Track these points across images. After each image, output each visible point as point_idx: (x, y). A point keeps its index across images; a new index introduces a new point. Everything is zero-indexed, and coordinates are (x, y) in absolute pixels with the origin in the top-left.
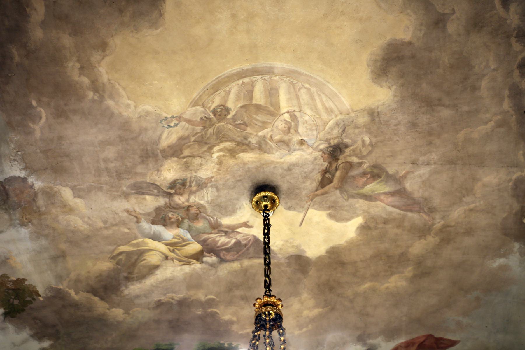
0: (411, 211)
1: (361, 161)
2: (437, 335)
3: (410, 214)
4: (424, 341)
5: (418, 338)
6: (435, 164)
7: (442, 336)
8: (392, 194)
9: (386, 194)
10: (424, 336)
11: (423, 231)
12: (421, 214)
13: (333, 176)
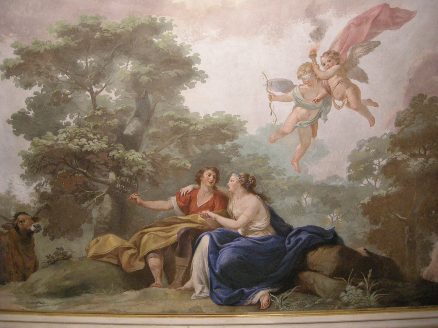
2: (392, 6)
5: (372, 10)
10: (379, 7)
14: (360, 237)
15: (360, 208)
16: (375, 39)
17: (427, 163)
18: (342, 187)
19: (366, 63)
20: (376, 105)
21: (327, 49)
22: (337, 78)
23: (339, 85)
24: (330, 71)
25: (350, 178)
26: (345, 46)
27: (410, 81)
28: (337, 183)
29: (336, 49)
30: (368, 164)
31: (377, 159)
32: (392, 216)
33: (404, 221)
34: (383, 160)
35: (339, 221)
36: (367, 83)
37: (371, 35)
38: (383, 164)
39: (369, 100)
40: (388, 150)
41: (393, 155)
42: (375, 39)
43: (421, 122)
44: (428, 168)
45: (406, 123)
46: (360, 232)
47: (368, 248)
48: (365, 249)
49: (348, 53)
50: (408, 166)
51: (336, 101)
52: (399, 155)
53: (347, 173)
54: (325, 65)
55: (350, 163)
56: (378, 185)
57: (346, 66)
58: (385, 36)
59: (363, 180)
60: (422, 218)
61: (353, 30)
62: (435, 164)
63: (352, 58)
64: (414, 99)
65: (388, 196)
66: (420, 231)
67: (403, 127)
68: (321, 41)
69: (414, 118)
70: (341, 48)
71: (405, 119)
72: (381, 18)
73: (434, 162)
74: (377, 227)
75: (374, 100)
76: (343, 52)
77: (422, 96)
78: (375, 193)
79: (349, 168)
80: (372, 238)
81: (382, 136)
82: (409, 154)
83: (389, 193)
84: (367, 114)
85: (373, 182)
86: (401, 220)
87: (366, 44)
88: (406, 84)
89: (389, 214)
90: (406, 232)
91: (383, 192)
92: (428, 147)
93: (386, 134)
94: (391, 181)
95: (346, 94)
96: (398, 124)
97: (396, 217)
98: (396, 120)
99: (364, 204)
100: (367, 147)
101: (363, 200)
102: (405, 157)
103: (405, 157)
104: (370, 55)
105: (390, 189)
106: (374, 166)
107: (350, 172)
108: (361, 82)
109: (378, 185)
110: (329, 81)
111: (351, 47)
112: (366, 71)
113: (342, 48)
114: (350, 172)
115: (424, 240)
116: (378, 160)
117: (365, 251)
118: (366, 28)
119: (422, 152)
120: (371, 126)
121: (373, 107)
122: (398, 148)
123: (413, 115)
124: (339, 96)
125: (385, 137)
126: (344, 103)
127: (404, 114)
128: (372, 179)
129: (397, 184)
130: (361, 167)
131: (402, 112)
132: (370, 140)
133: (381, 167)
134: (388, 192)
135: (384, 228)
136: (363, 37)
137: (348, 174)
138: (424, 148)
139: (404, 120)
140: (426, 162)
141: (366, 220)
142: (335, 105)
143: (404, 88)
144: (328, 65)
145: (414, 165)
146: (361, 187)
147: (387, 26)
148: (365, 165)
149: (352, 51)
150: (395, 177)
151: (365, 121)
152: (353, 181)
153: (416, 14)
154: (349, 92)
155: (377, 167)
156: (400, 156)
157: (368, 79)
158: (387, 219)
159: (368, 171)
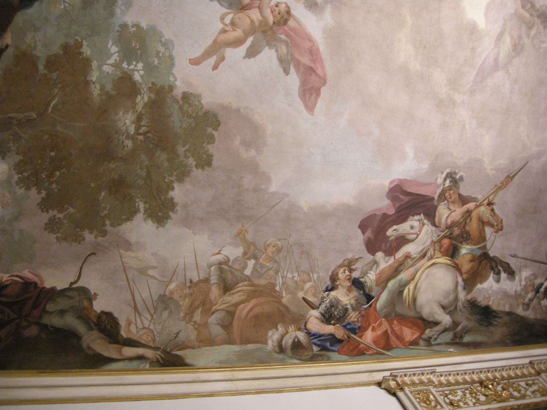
0: (477, 74)
1: (531, 37)
2: (323, 90)
3: (475, 72)
4: (317, 74)
5: (323, 68)
6: (510, 97)
7: (322, 95)
8: (496, 60)
9: (498, 54)
10: (325, 75)
11: (454, 83)
12: (471, 83)
13: (527, 11)
14: (29, 39)
15: (77, 40)
16: (292, 70)
17: (126, 138)
18: (112, 14)
19: (268, 57)
20: (215, 67)
21: (293, 12)
22: (258, 20)
23: (250, 22)
24: (268, 13)
25: (124, 26)
26: (292, 34)
27: (238, 110)
28: (120, 6)
29: (291, 23)
30: (139, 55)
31: (143, 67)
32: (56, 91)
33: (46, 110)
34: (141, 77)
35: (61, 5)
36: (244, 58)
37: (298, 65)
38: (135, 76)
39: (223, 59)
40: (153, 83)
41: (145, 89)
42: (292, 70)
43: (185, 125)
44: (119, 140)
45: (186, 107)
46: (37, 39)
47: (10, 51)
48: (7, 46)
49: (283, 37)
50: (126, 112)
51: (231, 16)
52: (143, 98)
53: (132, 22)
54: (277, 6)
55: (145, 28)
56: (106, 68)
57: (269, 33)
58: (294, 80)
59: (117, 46)
60: (46, 137)
61: (307, 45)
62: (123, 149)
63: (276, 40)
64: (215, 115)
65: (87, 83)
66: (26, 137)
67: (181, 102)
68: (303, 5)
69: (190, 116)
70: (294, 31)
71: (190, 105)
72: (313, 78)
73: (125, 148)
74: (41, 67)
75: (222, 65)
76: (285, 31)
77: (216, 125)
78: (95, 64)
79: (137, 26)
80: (26, 59)
81: (173, 74)
82: (143, 112)
83: (92, 84)
84: (206, 55)
85: (112, 61)
86: (48, 105)
87: (289, 58)
88: (235, 105)
89: (59, 86)
90: (27, 114)
91: (94, 76)
92: (148, 137)
93: (176, 80)
94: (109, 87)
95: (237, 29)
96: (186, 96)
97: (53, 98)
98: (191, 93)
99: (81, 46)
100: (163, 53)
101: (87, 46)
102: (139, 107)
103: (139, 107)
104: (276, 62)
105: (98, 86)
106: (134, 63)
107: (132, 27)
108: (248, 50)
109: (106, 68)
110: (257, 10)
111: (289, 41)
112: (259, 57)
113: (290, 29)
114: (132, 27)
115: (11, 144)
116: (141, 68)
117: (4, 47)
118: (305, 60)
119: (143, 129)
120: (190, 60)
121: (213, 64)
122: (153, 96)
123: (194, 115)
124: (237, 20)
125: (172, 79)
126: (226, 25)
127: (197, 103)
128: (116, 60)
129: (104, 97)
130: (136, 42)
131: (199, 101)
132: (171, 58)
133: (131, 73)
134: (94, 83)
135: (38, 79)
136: (297, 56)
137: (130, 24)
138: (148, 132)
139: (189, 104)
140: (128, 137)
141: (56, 49)
142: (227, 14)
143: (229, 103)
144: (275, 11)
145: (126, 121)
146: (108, 43)
147: (304, 83)
148: (138, 49)
149: (285, 41)
150: (114, 93)
151: (198, 52)
152: (118, 31)
153: (311, 115)
154: (238, 33)
155: (132, 67)
156: (142, 100)
157: (249, 58)
158: (52, 83)
159: (128, 54)
